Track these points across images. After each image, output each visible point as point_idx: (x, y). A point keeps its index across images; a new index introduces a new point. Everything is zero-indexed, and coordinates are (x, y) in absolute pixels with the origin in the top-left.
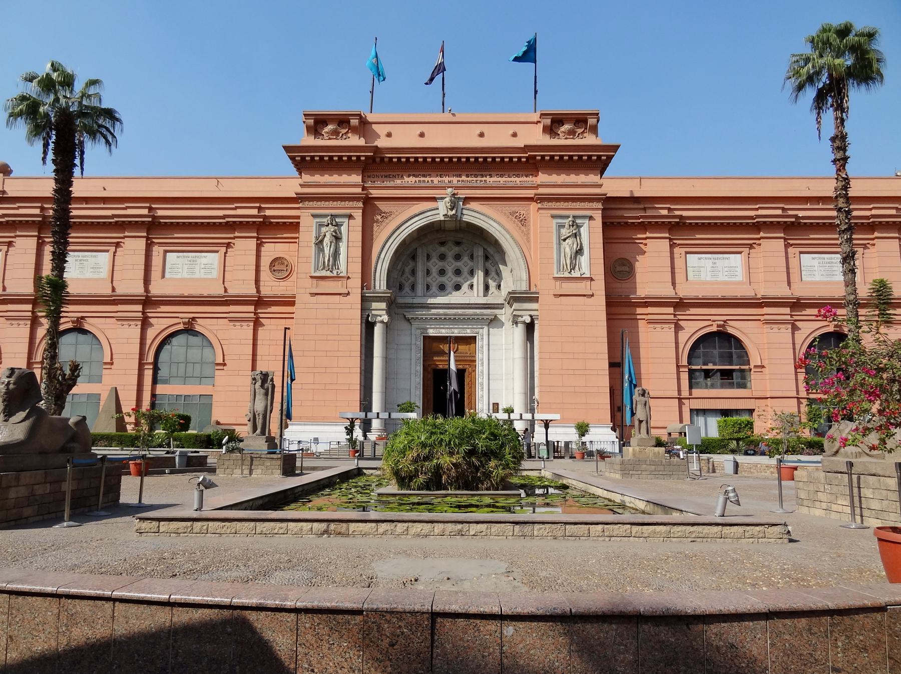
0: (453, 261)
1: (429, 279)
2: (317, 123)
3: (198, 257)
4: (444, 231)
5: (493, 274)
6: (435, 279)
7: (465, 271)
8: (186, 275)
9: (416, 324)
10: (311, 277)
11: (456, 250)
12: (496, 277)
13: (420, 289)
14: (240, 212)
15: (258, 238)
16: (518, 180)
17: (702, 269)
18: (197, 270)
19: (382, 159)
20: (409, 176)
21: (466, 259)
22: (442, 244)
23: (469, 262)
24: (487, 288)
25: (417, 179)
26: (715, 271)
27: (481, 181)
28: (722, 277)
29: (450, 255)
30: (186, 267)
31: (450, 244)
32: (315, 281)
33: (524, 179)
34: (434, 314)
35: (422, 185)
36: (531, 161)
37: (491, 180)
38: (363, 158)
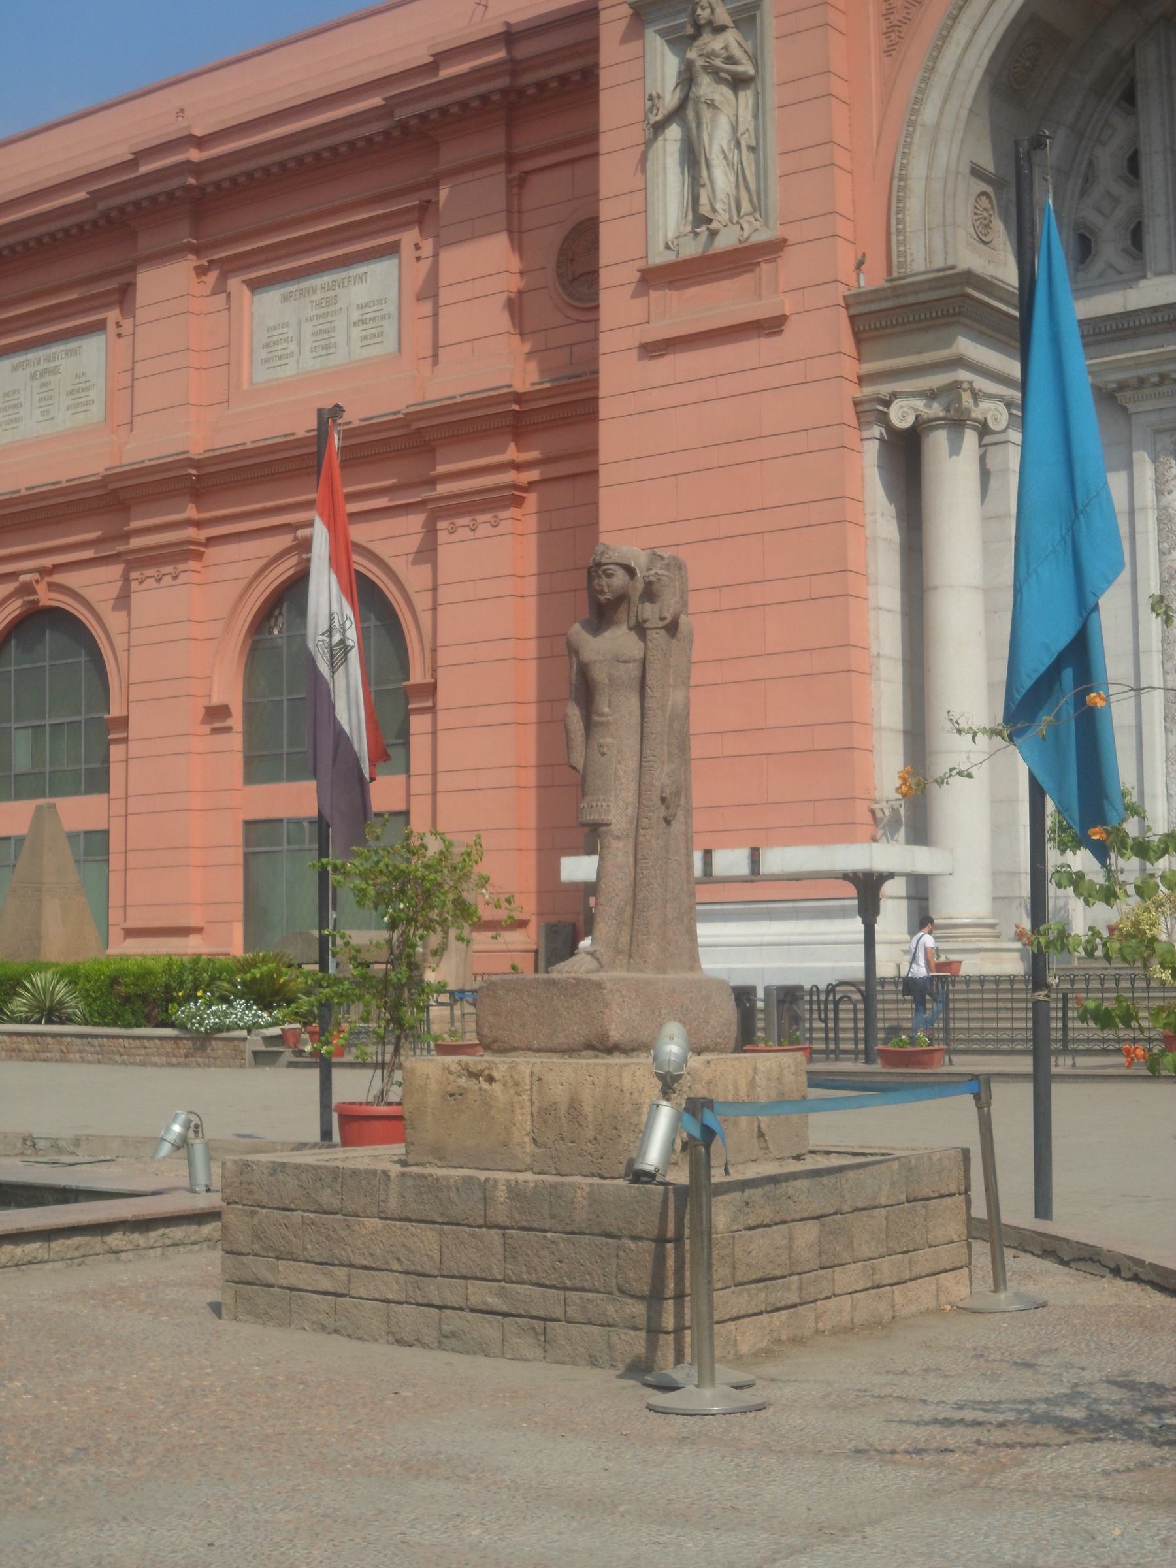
8: (310, 362)
15: (511, 159)
30: (308, 328)
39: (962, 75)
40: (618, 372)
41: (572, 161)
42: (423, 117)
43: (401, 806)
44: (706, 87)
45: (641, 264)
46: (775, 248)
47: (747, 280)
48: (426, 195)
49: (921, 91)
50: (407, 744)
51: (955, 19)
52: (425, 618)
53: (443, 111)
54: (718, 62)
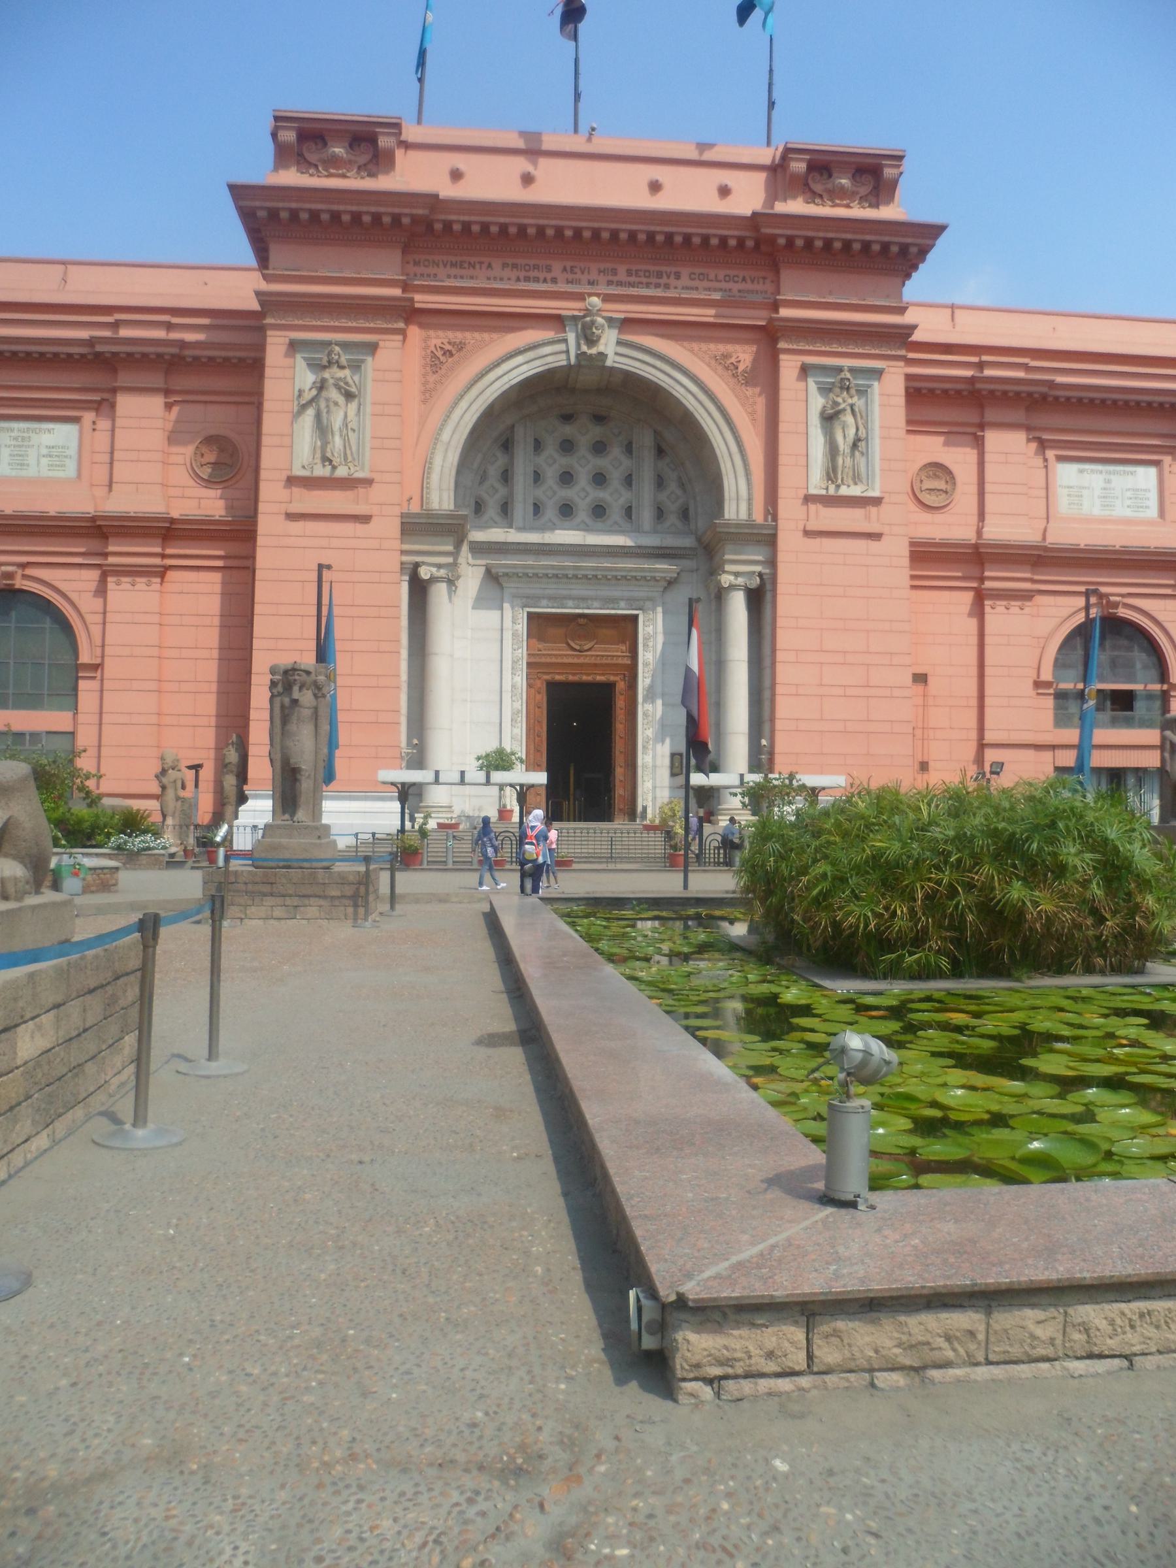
1: (539, 492)
2: (305, 138)
3: (34, 431)
4: (573, 391)
5: (673, 486)
6: (552, 493)
7: (616, 477)
9: (510, 587)
12: (679, 492)
13: (521, 509)
14: (124, 333)
16: (735, 287)
17: (1085, 492)
18: (32, 459)
19: (448, 226)
20: (505, 265)
21: (616, 451)
22: (567, 418)
24: (660, 513)
25: (522, 274)
28: (1122, 510)
29: (584, 441)
33: (749, 286)
34: (553, 567)
36: (763, 248)
39: (462, 423)
40: (268, 524)
41: (206, 402)
42: (115, 354)
43: (70, 729)
44: (334, 394)
45: (289, 473)
46: (368, 482)
47: (349, 493)
48: (106, 396)
49: (443, 425)
50: (76, 695)
51: (462, 396)
52: (96, 630)
53: (130, 355)
54: (342, 384)
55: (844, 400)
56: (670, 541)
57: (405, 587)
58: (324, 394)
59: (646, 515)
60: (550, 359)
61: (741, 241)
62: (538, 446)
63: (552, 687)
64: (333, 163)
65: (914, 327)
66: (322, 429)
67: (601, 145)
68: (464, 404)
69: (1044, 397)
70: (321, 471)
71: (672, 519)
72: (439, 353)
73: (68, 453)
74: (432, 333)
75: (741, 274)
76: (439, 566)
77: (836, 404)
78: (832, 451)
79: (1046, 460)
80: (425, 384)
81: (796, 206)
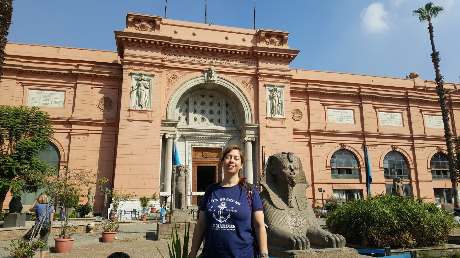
0: (209, 106)
4: (205, 89)
5: (230, 114)
10: (129, 110)
11: (210, 100)
12: (232, 116)
17: (335, 117)
18: (50, 102)
22: (203, 96)
23: (217, 107)
24: (227, 121)
26: (342, 118)
27: (228, 63)
28: (344, 122)
31: (207, 97)
32: (131, 113)
34: (200, 135)
35: (196, 62)
36: (254, 55)
37: (234, 63)
38: (163, 44)
46: (152, 111)
55: (276, 94)
56: (230, 129)
57: (161, 140)
58: (140, 87)
59: (224, 122)
60: (200, 81)
61: (249, 53)
62: (195, 103)
63: (198, 167)
64: (143, 27)
65: (292, 76)
66: (139, 97)
67: (213, 27)
68: (177, 92)
69: (324, 93)
70: (139, 108)
71: (230, 123)
72: (171, 78)
73: (61, 100)
74: (169, 73)
75: (249, 61)
76: (170, 135)
77: (273, 94)
78: (273, 106)
79: (325, 109)
80: (167, 86)
81: (262, 44)
